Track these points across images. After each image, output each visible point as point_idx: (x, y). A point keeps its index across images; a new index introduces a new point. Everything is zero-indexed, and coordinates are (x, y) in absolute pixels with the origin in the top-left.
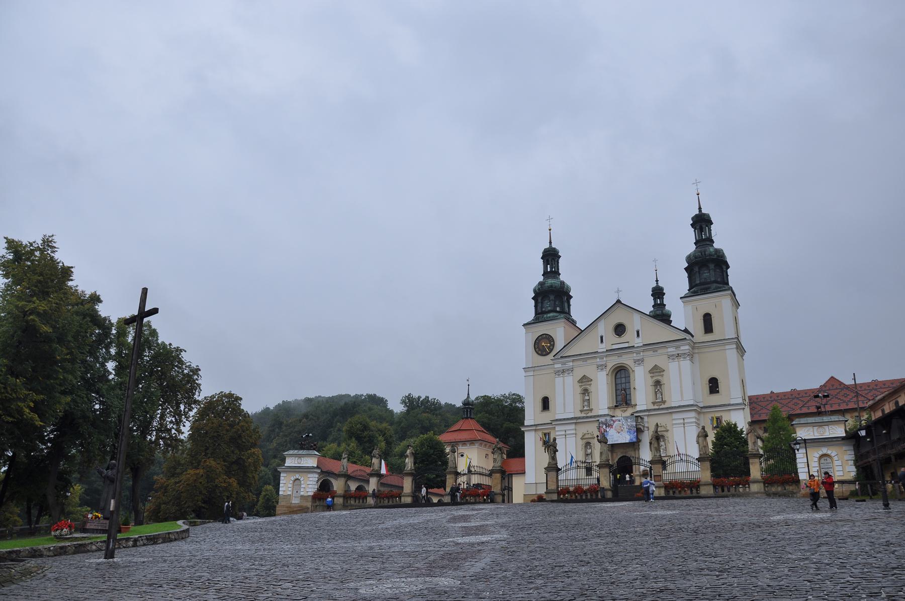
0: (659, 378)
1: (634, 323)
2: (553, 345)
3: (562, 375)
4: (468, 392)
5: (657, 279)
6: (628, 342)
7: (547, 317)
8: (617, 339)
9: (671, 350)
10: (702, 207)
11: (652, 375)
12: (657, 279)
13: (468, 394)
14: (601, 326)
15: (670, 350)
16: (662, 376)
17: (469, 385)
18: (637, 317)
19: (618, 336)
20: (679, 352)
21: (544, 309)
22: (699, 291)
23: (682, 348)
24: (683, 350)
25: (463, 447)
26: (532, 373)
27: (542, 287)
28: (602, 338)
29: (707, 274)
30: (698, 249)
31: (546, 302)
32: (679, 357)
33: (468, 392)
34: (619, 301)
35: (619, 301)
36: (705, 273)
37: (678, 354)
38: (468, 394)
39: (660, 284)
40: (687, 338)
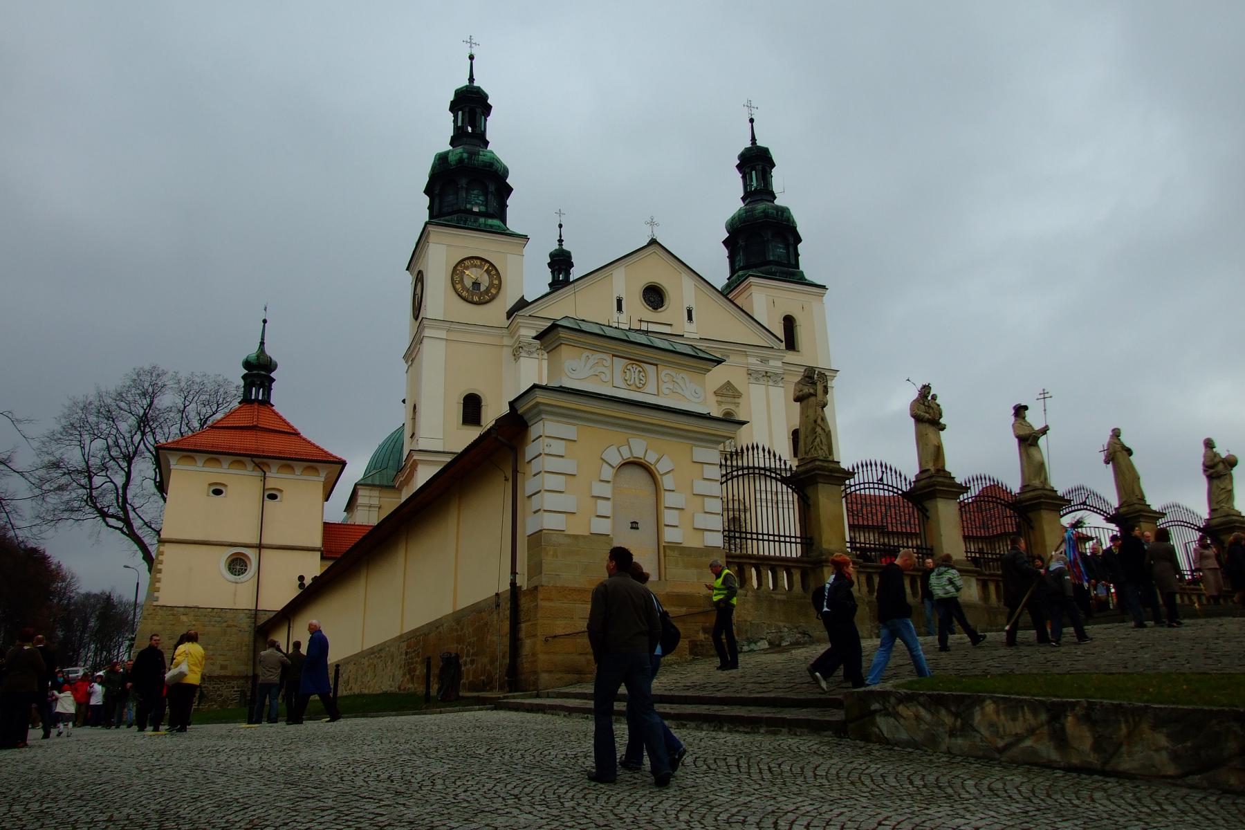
0: (732, 407)
1: (682, 293)
2: (499, 287)
3: (535, 355)
4: (263, 339)
5: (560, 236)
6: (671, 325)
7: (486, 225)
8: (647, 313)
9: (753, 361)
10: (756, 138)
11: (719, 399)
12: (560, 236)
13: (262, 343)
14: (619, 274)
15: (752, 360)
16: (737, 405)
17: (265, 321)
18: (688, 283)
19: (651, 308)
20: (767, 369)
21: (469, 206)
22: (778, 274)
23: (772, 363)
24: (772, 367)
25: (277, 475)
26: (443, 334)
27: (470, 158)
28: (619, 302)
29: (781, 250)
30: (748, 207)
31: (475, 192)
32: (765, 378)
33: (263, 339)
34: (653, 242)
35: (653, 242)
36: (780, 248)
37: (766, 372)
38: (262, 343)
39: (566, 247)
40: (775, 347)
